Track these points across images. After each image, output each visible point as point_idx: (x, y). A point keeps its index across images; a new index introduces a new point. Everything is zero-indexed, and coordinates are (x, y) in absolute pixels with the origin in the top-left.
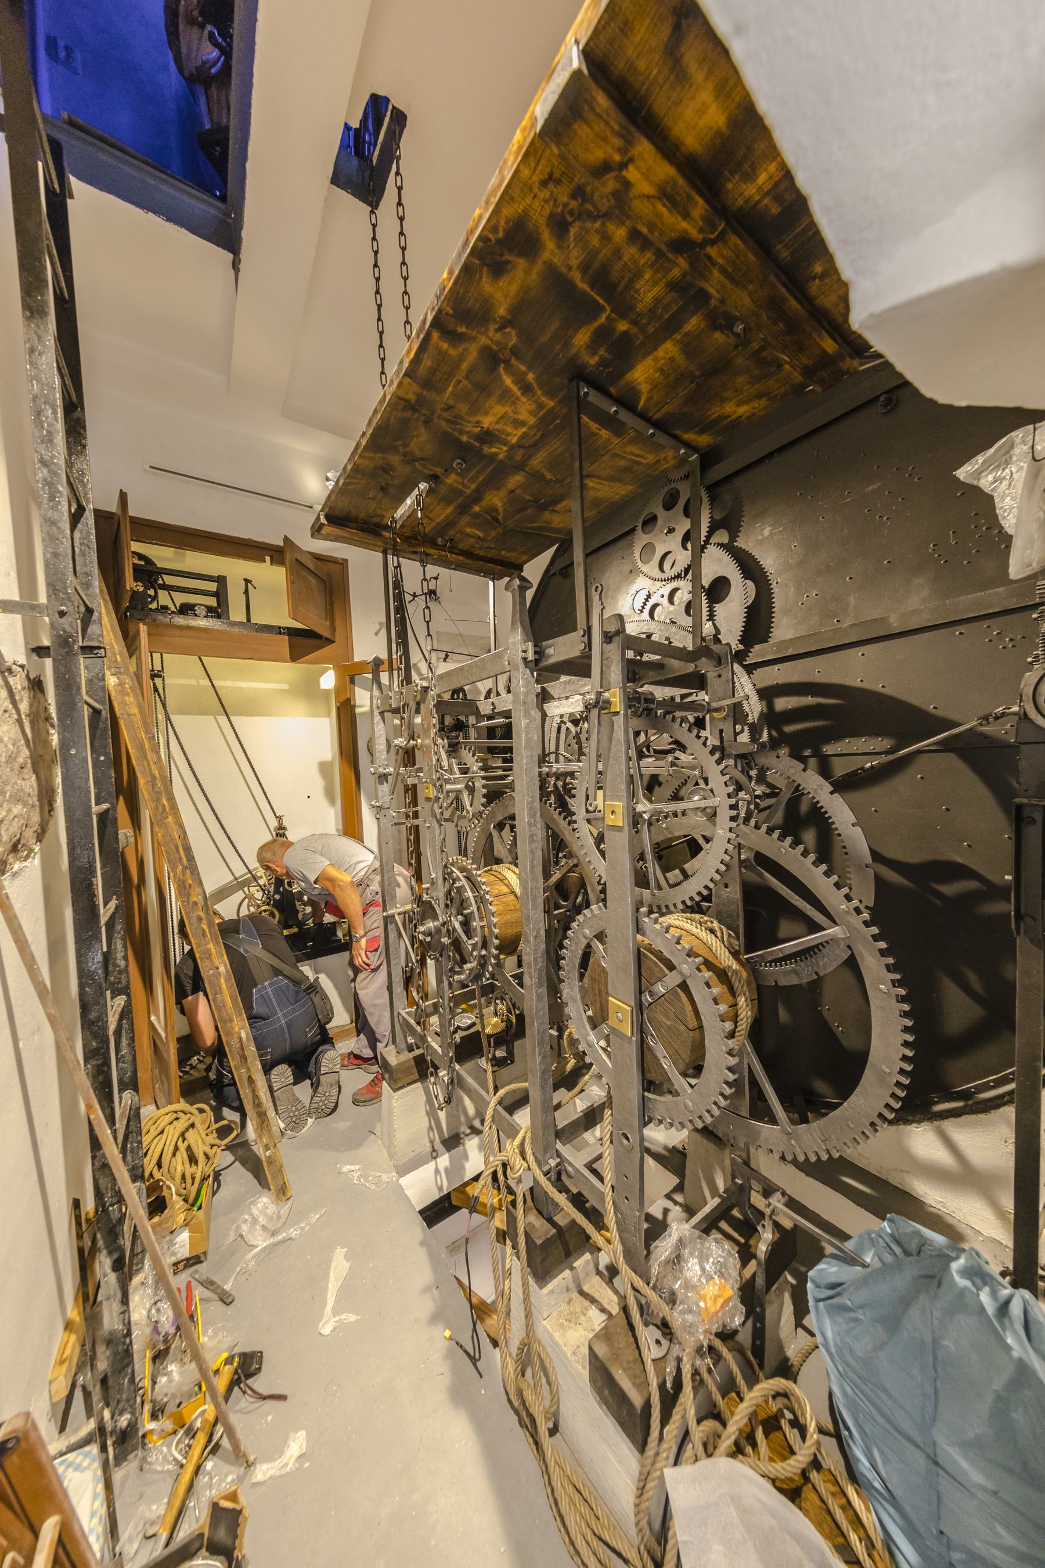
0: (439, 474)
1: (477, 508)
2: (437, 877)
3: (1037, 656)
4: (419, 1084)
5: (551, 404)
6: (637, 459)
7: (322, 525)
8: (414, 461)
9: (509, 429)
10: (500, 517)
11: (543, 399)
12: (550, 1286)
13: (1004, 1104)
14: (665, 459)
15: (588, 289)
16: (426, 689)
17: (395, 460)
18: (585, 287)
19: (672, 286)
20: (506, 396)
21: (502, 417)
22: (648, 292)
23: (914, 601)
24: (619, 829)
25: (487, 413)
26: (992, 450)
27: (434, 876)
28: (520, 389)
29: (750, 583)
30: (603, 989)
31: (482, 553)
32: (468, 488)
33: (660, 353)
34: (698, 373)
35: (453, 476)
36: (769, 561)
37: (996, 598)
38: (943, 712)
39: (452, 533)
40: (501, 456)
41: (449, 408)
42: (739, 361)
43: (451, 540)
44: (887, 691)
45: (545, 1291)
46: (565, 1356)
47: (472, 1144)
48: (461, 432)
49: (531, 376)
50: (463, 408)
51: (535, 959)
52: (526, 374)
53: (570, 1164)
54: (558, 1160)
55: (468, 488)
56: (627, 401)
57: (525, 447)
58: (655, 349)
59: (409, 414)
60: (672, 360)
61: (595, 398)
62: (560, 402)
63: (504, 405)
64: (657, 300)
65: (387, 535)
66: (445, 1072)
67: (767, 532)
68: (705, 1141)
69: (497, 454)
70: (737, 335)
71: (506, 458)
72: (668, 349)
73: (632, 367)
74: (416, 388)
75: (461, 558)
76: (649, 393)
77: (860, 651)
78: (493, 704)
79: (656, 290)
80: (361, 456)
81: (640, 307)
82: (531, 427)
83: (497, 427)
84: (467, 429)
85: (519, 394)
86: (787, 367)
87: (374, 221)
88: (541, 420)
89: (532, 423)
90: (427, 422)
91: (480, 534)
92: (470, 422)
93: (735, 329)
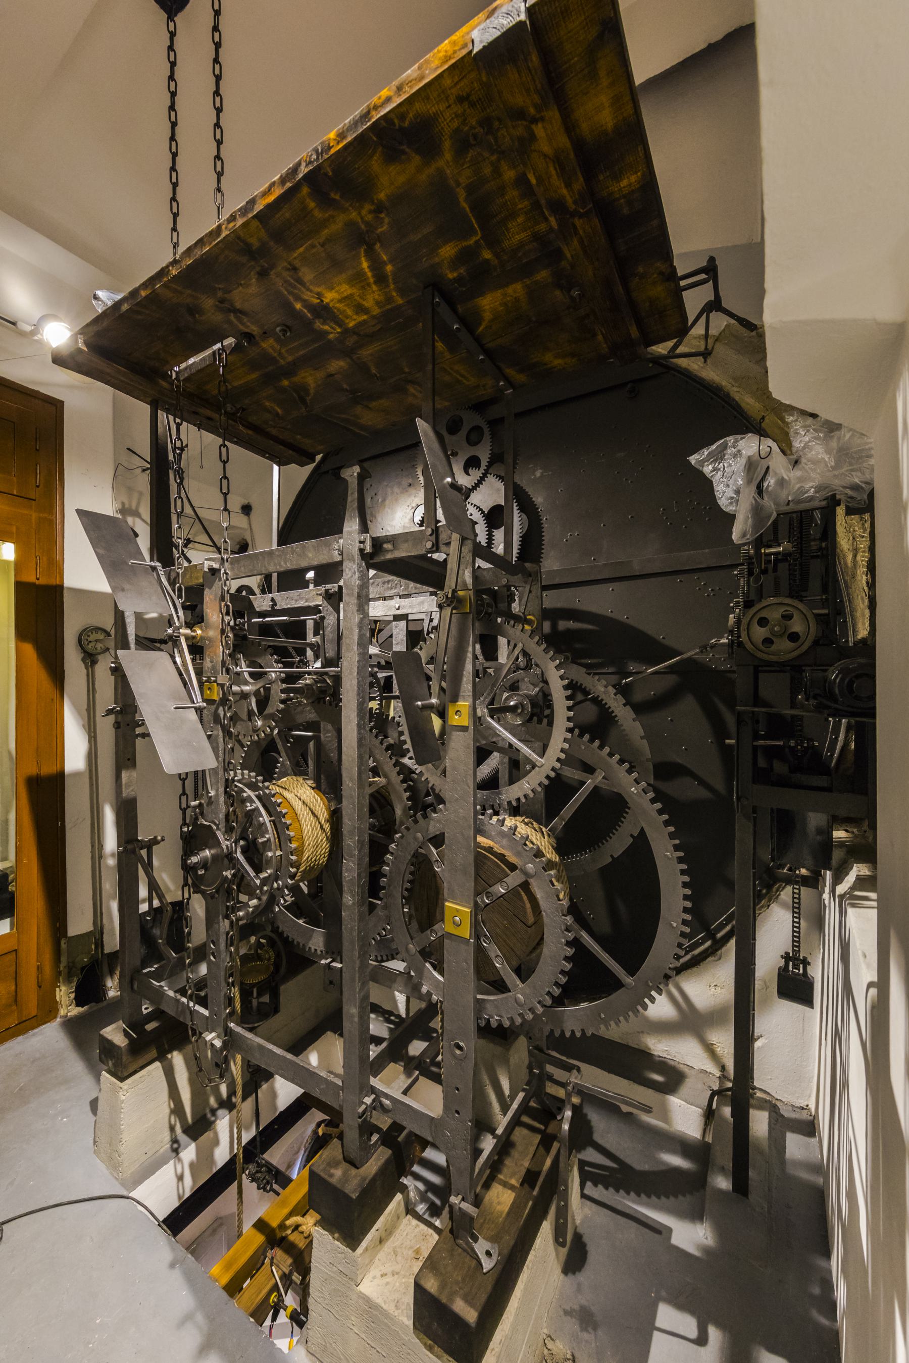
1: (286, 383)
2: (217, 795)
3: (738, 602)
4: (157, 1064)
5: (400, 301)
6: (460, 378)
7: (80, 351)
8: (230, 311)
9: (349, 312)
10: (308, 399)
11: (394, 294)
12: (364, 1244)
14: (484, 386)
15: (468, 209)
16: (213, 572)
17: (208, 303)
18: (465, 205)
19: (536, 237)
21: (346, 297)
22: (516, 234)
23: (647, 554)
24: (464, 729)
25: (331, 288)
26: (714, 447)
27: (212, 793)
28: (374, 276)
29: (524, 516)
32: (283, 358)
33: (510, 290)
34: (534, 319)
35: (271, 341)
36: (539, 499)
37: (704, 556)
38: (670, 642)
40: (331, 336)
43: (244, 410)
44: (631, 622)
45: (360, 1250)
46: (386, 1314)
47: (223, 1124)
48: (298, 298)
51: (359, 875)
52: (385, 264)
53: (387, 1096)
54: (373, 1096)
56: (469, 323)
58: (507, 285)
59: (244, 259)
60: (517, 300)
61: (444, 310)
63: (353, 286)
65: (164, 384)
66: (214, 1034)
67: (538, 474)
68: (491, 1045)
69: (328, 333)
71: (336, 339)
72: (516, 290)
74: (263, 234)
75: (250, 432)
77: (610, 587)
78: (273, 600)
79: (523, 235)
80: (165, 286)
81: (506, 244)
82: (374, 317)
83: (337, 305)
84: (306, 297)
85: (371, 280)
87: (172, 28)
89: (374, 313)
91: (279, 411)
92: (308, 290)
93: (572, 293)
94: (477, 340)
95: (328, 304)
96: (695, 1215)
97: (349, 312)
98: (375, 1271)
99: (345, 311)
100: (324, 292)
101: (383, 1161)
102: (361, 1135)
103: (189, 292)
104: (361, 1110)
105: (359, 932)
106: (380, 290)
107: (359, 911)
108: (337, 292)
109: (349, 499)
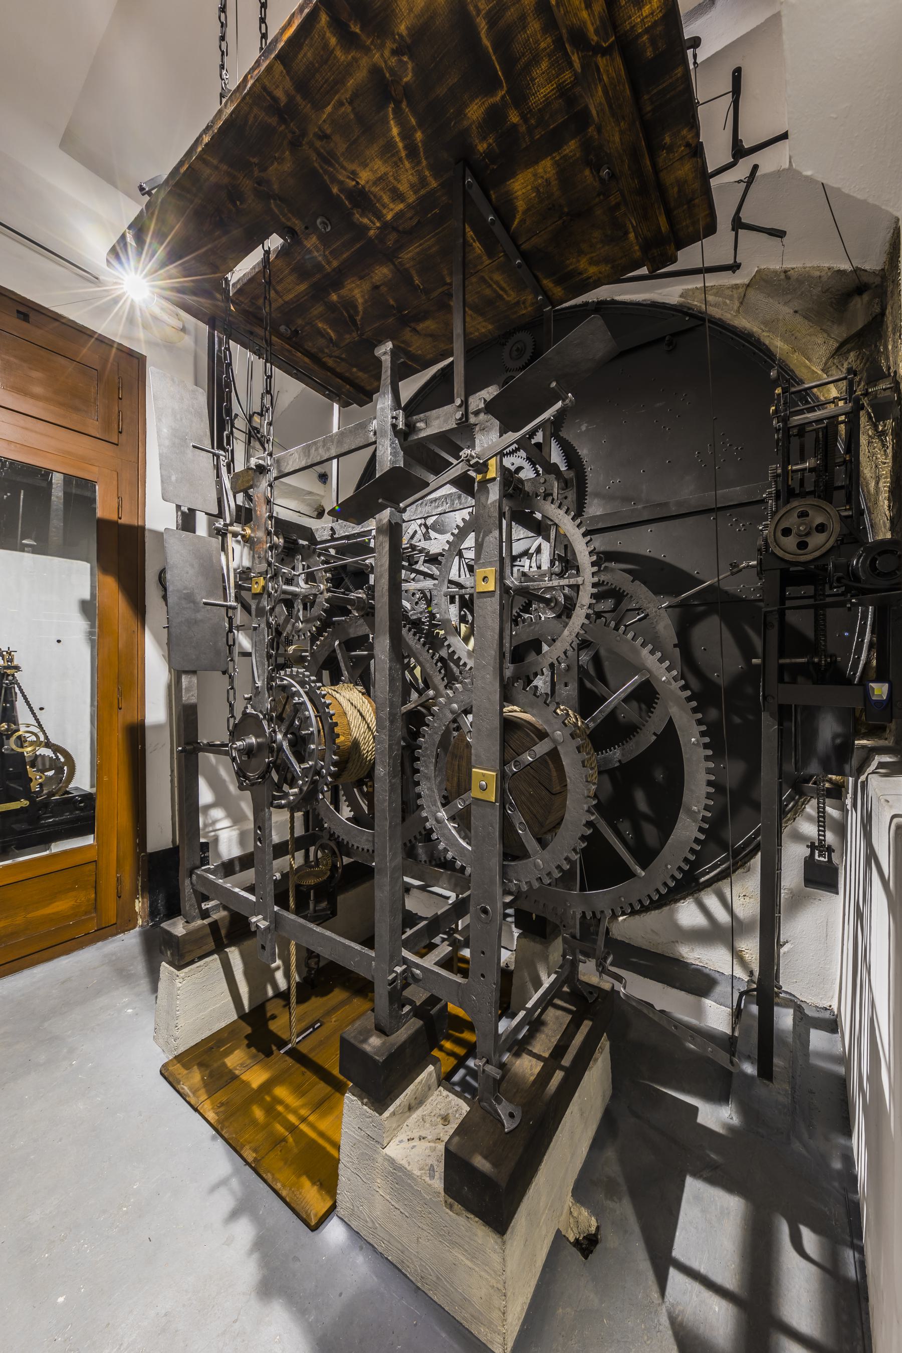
0: (297, 229)
5: (434, 184)
11: (427, 173)
20: (389, 148)
25: (365, 165)
30: (464, 764)
41: (324, 137)
48: (334, 179)
49: (419, 135)
50: (340, 146)
51: (390, 746)
53: (418, 966)
54: (404, 967)
61: (476, 192)
64: (548, 103)
70: (602, 180)
83: (373, 189)
84: (341, 178)
88: (421, 200)
95: (363, 187)
96: (720, 1097)
98: (403, 1135)
99: (381, 197)
101: (410, 1032)
102: (391, 1002)
104: (390, 978)
105: (390, 803)
106: (413, 168)
107: (390, 781)
108: (371, 170)
109: (383, 377)
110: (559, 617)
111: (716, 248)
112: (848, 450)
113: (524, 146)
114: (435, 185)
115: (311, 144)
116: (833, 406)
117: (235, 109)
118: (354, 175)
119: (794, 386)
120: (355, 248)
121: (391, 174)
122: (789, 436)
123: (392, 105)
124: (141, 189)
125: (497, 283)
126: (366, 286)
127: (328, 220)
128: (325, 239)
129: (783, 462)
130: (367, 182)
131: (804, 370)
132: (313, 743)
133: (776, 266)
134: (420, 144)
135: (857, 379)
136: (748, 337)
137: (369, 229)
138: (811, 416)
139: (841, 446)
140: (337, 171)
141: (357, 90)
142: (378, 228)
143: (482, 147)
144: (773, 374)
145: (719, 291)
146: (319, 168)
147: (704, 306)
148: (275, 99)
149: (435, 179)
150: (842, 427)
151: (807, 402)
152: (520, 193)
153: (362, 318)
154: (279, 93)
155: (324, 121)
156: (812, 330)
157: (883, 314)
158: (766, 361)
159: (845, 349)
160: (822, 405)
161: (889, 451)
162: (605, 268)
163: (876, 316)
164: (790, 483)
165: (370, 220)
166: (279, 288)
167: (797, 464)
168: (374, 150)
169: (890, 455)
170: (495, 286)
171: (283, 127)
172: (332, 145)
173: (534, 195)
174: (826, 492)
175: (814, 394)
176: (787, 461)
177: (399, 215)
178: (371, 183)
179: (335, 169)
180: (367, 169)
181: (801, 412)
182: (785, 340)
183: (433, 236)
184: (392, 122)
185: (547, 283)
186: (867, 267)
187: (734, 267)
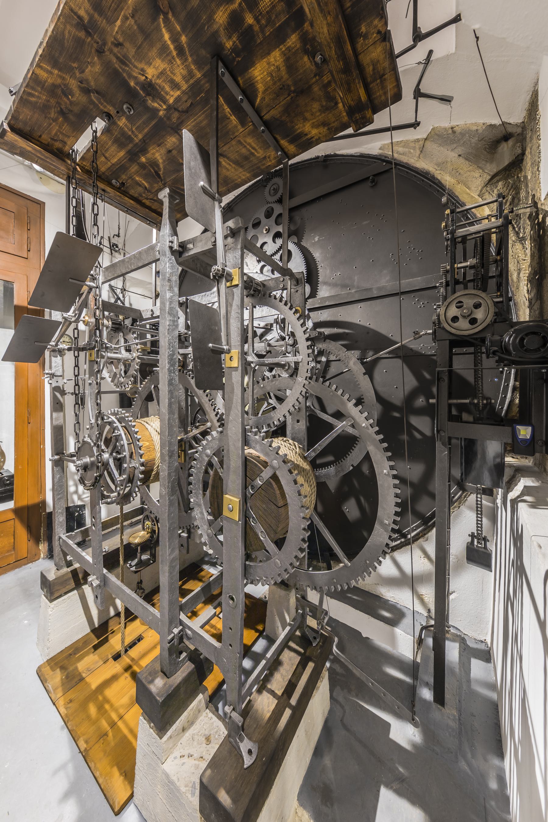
0: (111, 113)
5: (199, 75)
9: (167, 88)
11: (193, 67)
13: (420, 538)
20: (164, 49)
25: (149, 64)
28: (176, 48)
31: (147, 203)
34: (292, 88)
39: (124, 177)
42: (316, 89)
48: (130, 76)
49: (184, 39)
50: (130, 50)
55: (136, 136)
56: (249, 92)
57: (179, 111)
62: (204, 75)
71: (165, 116)
73: (252, 64)
76: (264, 92)
82: (184, 92)
83: (158, 81)
84: (135, 74)
86: (340, 105)
90: (100, 52)
92: (137, 68)
94: (258, 112)
95: (151, 80)
97: (167, 88)
99: (164, 86)
100: (145, 67)
103: (56, 72)
110: (291, 376)
111: (402, 111)
112: (498, 253)
113: (259, 41)
114: (199, 76)
115: (111, 51)
116: (487, 221)
117: (55, 27)
118: (143, 72)
119: (458, 208)
120: (152, 125)
121: (168, 69)
122: (455, 244)
123: (162, 17)
124: (11, 92)
125: (249, 144)
126: (163, 151)
127: (131, 105)
128: (129, 118)
129: (451, 262)
130: (153, 76)
131: (465, 196)
132: (126, 463)
133: (446, 124)
134: (185, 45)
135: (504, 201)
136: (426, 175)
137: (159, 111)
138: (472, 229)
139: (493, 250)
140: (132, 70)
141: (136, 6)
142: (165, 110)
143: (229, 44)
144: (444, 200)
145: (405, 144)
146: (119, 68)
147: (391, 153)
148: (80, 17)
149: (199, 71)
150: (494, 237)
151: (468, 219)
152: (259, 78)
153: (163, 173)
154: (82, 13)
155: (117, 32)
156: (471, 168)
157: (523, 154)
158: (438, 191)
159: (495, 180)
160: (479, 221)
161: (528, 252)
162: (324, 130)
163: (518, 155)
164: (456, 277)
165: (158, 104)
166: (107, 155)
167: (461, 263)
168: (154, 52)
169: (529, 254)
170: (248, 147)
171: (89, 39)
172: (125, 50)
173: (269, 78)
174: (482, 283)
175: (473, 213)
176: (453, 261)
177: (178, 99)
178: (155, 77)
179: (130, 68)
180: (152, 67)
181: (464, 226)
182: (452, 176)
183: (203, 113)
184: (164, 30)
185: (284, 143)
186: (512, 121)
187: (415, 125)
